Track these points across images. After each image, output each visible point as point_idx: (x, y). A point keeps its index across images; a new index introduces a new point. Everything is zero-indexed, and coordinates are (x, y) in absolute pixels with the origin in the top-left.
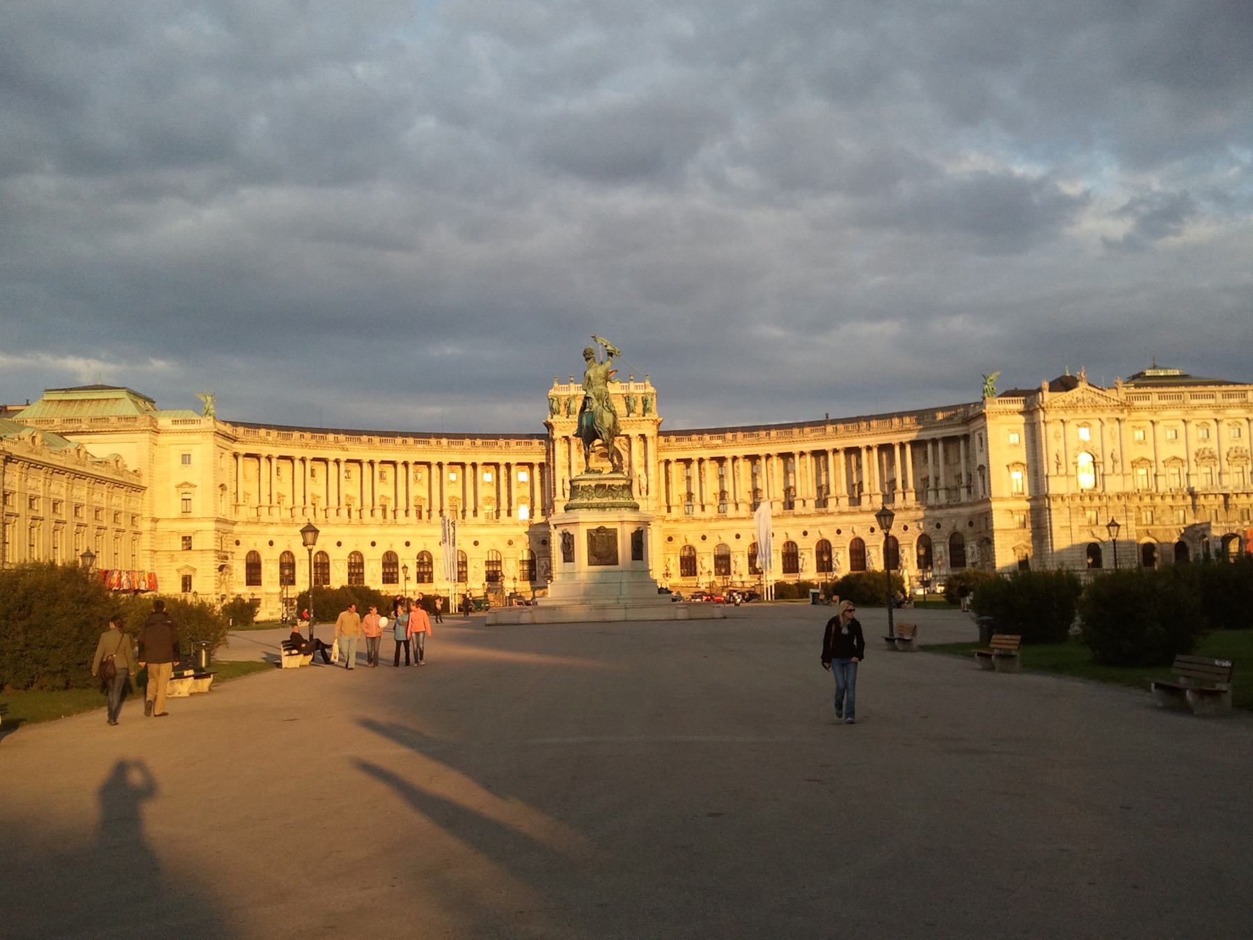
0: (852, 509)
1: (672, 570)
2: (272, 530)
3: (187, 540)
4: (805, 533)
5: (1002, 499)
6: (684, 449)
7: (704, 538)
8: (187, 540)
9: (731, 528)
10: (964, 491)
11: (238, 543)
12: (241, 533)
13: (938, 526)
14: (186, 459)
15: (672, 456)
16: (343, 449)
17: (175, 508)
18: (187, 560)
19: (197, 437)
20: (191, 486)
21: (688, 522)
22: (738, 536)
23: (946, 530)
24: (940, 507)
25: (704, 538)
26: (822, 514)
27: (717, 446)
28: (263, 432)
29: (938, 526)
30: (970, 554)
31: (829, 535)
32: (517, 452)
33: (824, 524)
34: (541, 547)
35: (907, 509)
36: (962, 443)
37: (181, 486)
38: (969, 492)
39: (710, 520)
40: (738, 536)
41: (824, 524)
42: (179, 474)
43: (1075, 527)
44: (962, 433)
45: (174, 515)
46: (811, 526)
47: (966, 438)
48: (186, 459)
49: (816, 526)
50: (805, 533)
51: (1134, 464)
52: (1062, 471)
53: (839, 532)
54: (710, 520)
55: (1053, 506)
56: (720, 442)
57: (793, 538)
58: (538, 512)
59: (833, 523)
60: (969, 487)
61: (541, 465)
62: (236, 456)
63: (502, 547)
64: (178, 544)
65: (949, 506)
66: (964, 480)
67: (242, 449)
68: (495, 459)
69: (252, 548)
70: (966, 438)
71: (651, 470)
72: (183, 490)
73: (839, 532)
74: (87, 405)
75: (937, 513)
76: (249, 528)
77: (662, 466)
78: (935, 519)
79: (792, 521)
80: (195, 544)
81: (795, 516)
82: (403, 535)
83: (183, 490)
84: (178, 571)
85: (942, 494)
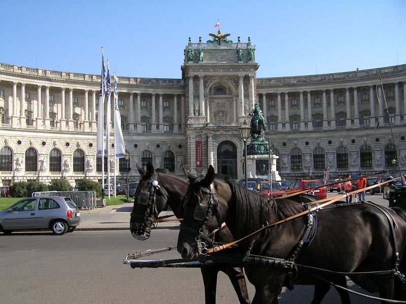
4: (353, 141)
9: (303, 138)
15: (264, 91)
22: (307, 143)
25: (284, 144)
27: (293, 85)
31: (371, 143)
33: (367, 135)
34: (178, 150)
39: (289, 133)
40: (307, 143)
46: (358, 137)
49: (361, 136)
50: (353, 141)
54: (289, 133)
57: (345, 144)
58: (176, 127)
59: (373, 135)
61: (179, 96)
63: (152, 149)
68: (150, 91)
73: (377, 140)
79: (345, 133)
81: (348, 130)
82: (88, 139)
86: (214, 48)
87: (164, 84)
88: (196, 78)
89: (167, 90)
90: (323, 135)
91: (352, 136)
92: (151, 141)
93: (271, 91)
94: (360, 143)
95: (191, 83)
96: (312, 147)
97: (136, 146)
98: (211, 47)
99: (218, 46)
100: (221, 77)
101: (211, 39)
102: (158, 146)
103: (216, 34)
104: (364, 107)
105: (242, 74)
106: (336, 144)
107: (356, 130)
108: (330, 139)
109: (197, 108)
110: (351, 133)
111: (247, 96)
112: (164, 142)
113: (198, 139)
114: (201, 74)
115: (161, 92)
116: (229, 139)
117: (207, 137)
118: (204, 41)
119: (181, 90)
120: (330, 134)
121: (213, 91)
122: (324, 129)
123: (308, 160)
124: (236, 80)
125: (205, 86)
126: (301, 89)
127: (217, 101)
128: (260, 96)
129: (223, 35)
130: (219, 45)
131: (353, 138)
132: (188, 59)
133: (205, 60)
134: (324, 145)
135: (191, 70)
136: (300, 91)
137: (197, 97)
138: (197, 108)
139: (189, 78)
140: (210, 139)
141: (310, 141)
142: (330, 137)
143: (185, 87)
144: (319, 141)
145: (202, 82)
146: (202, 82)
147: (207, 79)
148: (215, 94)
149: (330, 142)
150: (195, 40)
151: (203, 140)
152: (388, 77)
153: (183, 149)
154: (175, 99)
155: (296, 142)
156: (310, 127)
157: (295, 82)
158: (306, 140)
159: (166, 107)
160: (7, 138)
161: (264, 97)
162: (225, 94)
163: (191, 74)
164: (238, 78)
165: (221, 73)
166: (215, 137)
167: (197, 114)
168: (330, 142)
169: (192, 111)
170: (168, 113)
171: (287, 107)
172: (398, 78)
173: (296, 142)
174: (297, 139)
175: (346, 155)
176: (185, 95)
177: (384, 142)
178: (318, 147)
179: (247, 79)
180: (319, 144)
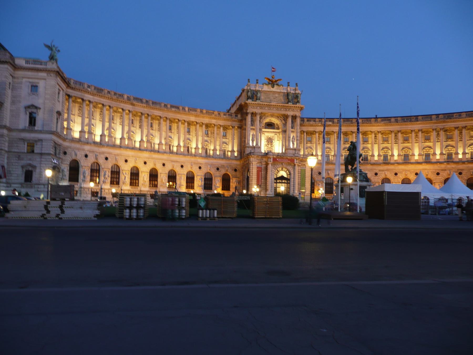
4: (376, 174)
6: (312, 125)
8: (31, 146)
11: (65, 153)
12: (68, 147)
16: (132, 104)
18: (30, 160)
19: (43, 74)
20: (36, 108)
32: (224, 120)
33: (388, 170)
34: (234, 173)
37: (27, 107)
41: (388, 170)
42: (26, 98)
45: (21, 126)
46: (380, 170)
48: (34, 88)
49: (383, 170)
56: (331, 123)
63: (213, 172)
64: (24, 148)
69: (74, 157)
72: (30, 110)
75: (461, 166)
78: (458, 170)
80: (37, 149)
82: (162, 159)
83: (30, 110)
84: (22, 167)
86: (269, 90)
87: (225, 117)
88: (253, 114)
89: (227, 122)
92: (212, 165)
95: (249, 118)
99: (272, 89)
102: (218, 169)
103: (271, 78)
112: (223, 166)
113: (258, 165)
114: (258, 111)
117: (267, 164)
119: (239, 123)
127: (267, 134)
129: (276, 78)
130: (273, 87)
135: (250, 107)
139: (247, 114)
145: (258, 117)
151: (263, 166)
153: (238, 173)
162: (274, 129)
163: (250, 110)
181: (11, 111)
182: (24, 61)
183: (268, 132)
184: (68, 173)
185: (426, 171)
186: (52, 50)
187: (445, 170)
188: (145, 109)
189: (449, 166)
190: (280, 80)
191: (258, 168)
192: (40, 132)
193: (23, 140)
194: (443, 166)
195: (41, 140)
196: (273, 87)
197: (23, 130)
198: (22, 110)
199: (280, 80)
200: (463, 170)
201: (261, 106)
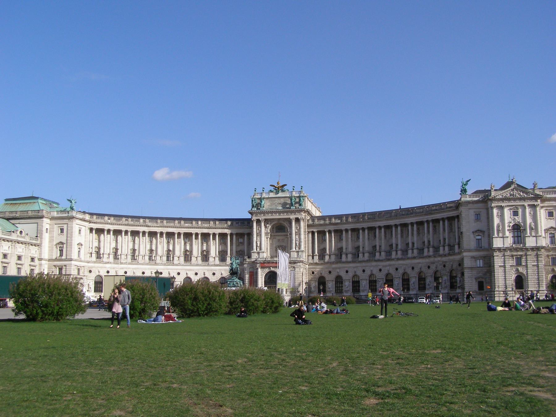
0: (403, 257)
1: (313, 289)
2: (108, 266)
3: (60, 269)
4: (380, 270)
5: (469, 251)
7: (330, 272)
8: (60, 269)
9: (344, 267)
10: (456, 247)
11: (90, 271)
13: (444, 266)
14: (62, 230)
17: (56, 253)
21: (322, 264)
22: (347, 272)
23: (448, 269)
24: (445, 255)
25: (330, 272)
26: (389, 260)
28: (106, 218)
29: (444, 266)
30: (458, 282)
33: (390, 265)
35: (430, 257)
36: (456, 220)
37: (58, 244)
38: (459, 247)
40: (347, 272)
43: (508, 266)
44: (456, 215)
46: (383, 266)
47: (458, 217)
48: (62, 230)
49: (386, 266)
50: (380, 270)
51: (546, 230)
52: (501, 235)
53: (397, 269)
55: (495, 254)
57: (374, 272)
59: (394, 265)
60: (459, 244)
62: (91, 230)
65: (449, 255)
66: (457, 241)
67: (95, 226)
69: (98, 274)
70: (458, 217)
71: (302, 237)
73: (397, 269)
74: (21, 205)
75: (444, 259)
76: (96, 265)
77: (310, 235)
78: (443, 262)
79: (374, 263)
85: (447, 248)
90: (358, 265)
91: (379, 265)
93: (321, 229)
94: (384, 272)
96: (351, 274)
97: (214, 274)
98: (272, 195)
100: (280, 219)
101: (272, 188)
104: (357, 244)
105: (293, 217)
106: (368, 272)
107: (382, 261)
108: (364, 268)
109: (259, 245)
110: (379, 263)
111: (298, 233)
114: (262, 217)
115: (235, 231)
116: (272, 269)
118: (267, 190)
120: (364, 264)
121: (275, 230)
122: (360, 259)
123: (347, 285)
124: (289, 221)
125: (266, 227)
126: (343, 227)
127: (278, 238)
128: (313, 233)
129: (281, 185)
131: (380, 267)
132: (253, 206)
133: (266, 205)
134: (360, 273)
136: (343, 228)
137: (259, 234)
138: (259, 245)
140: (259, 270)
141: (349, 270)
142: (364, 266)
143: (252, 227)
144: (355, 269)
145: (263, 224)
146: (263, 224)
147: (267, 221)
148: (277, 232)
149: (364, 271)
150: (259, 190)
152: (403, 218)
154: (246, 236)
155: (338, 270)
156: (350, 257)
157: (339, 221)
158: (346, 269)
159: (241, 243)
160: (117, 270)
161: (316, 234)
162: (284, 232)
164: (289, 221)
165: (277, 216)
166: (262, 267)
167: (258, 249)
168: (364, 271)
169: (255, 247)
170: (240, 248)
171: (350, 240)
172: (411, 219)
173: (338, 270)
174: (340, 268)
175: (375, 281)
176: (250, 235)
177: (401, 271)
178: (355, 276)
179: (297, 220)
180: (355, 272)
181: (49, 247)
182: (56, 213)
183: (279, 236)
184: (94, 286)
185: (420, 265)
186: (71, 202)
187: (434, 263)
188: (160, 229)
189: (436, 259)
190: (286, 185)
191: (250, 272)
192: (65, 260)
193: (55, 266)
194: (432, 259)
195: (65, 266)
196: (277, 193)
197: (56, 260)
198: (55, 247)
199: (286, 185)
200: (446, 262)
201: (264, 213)
